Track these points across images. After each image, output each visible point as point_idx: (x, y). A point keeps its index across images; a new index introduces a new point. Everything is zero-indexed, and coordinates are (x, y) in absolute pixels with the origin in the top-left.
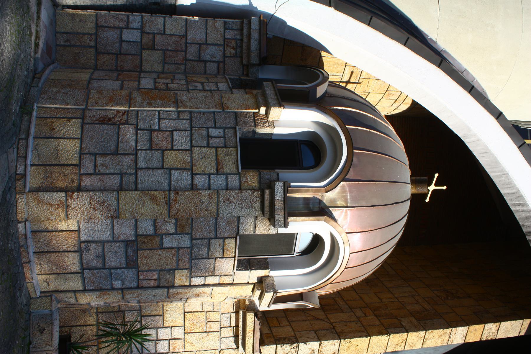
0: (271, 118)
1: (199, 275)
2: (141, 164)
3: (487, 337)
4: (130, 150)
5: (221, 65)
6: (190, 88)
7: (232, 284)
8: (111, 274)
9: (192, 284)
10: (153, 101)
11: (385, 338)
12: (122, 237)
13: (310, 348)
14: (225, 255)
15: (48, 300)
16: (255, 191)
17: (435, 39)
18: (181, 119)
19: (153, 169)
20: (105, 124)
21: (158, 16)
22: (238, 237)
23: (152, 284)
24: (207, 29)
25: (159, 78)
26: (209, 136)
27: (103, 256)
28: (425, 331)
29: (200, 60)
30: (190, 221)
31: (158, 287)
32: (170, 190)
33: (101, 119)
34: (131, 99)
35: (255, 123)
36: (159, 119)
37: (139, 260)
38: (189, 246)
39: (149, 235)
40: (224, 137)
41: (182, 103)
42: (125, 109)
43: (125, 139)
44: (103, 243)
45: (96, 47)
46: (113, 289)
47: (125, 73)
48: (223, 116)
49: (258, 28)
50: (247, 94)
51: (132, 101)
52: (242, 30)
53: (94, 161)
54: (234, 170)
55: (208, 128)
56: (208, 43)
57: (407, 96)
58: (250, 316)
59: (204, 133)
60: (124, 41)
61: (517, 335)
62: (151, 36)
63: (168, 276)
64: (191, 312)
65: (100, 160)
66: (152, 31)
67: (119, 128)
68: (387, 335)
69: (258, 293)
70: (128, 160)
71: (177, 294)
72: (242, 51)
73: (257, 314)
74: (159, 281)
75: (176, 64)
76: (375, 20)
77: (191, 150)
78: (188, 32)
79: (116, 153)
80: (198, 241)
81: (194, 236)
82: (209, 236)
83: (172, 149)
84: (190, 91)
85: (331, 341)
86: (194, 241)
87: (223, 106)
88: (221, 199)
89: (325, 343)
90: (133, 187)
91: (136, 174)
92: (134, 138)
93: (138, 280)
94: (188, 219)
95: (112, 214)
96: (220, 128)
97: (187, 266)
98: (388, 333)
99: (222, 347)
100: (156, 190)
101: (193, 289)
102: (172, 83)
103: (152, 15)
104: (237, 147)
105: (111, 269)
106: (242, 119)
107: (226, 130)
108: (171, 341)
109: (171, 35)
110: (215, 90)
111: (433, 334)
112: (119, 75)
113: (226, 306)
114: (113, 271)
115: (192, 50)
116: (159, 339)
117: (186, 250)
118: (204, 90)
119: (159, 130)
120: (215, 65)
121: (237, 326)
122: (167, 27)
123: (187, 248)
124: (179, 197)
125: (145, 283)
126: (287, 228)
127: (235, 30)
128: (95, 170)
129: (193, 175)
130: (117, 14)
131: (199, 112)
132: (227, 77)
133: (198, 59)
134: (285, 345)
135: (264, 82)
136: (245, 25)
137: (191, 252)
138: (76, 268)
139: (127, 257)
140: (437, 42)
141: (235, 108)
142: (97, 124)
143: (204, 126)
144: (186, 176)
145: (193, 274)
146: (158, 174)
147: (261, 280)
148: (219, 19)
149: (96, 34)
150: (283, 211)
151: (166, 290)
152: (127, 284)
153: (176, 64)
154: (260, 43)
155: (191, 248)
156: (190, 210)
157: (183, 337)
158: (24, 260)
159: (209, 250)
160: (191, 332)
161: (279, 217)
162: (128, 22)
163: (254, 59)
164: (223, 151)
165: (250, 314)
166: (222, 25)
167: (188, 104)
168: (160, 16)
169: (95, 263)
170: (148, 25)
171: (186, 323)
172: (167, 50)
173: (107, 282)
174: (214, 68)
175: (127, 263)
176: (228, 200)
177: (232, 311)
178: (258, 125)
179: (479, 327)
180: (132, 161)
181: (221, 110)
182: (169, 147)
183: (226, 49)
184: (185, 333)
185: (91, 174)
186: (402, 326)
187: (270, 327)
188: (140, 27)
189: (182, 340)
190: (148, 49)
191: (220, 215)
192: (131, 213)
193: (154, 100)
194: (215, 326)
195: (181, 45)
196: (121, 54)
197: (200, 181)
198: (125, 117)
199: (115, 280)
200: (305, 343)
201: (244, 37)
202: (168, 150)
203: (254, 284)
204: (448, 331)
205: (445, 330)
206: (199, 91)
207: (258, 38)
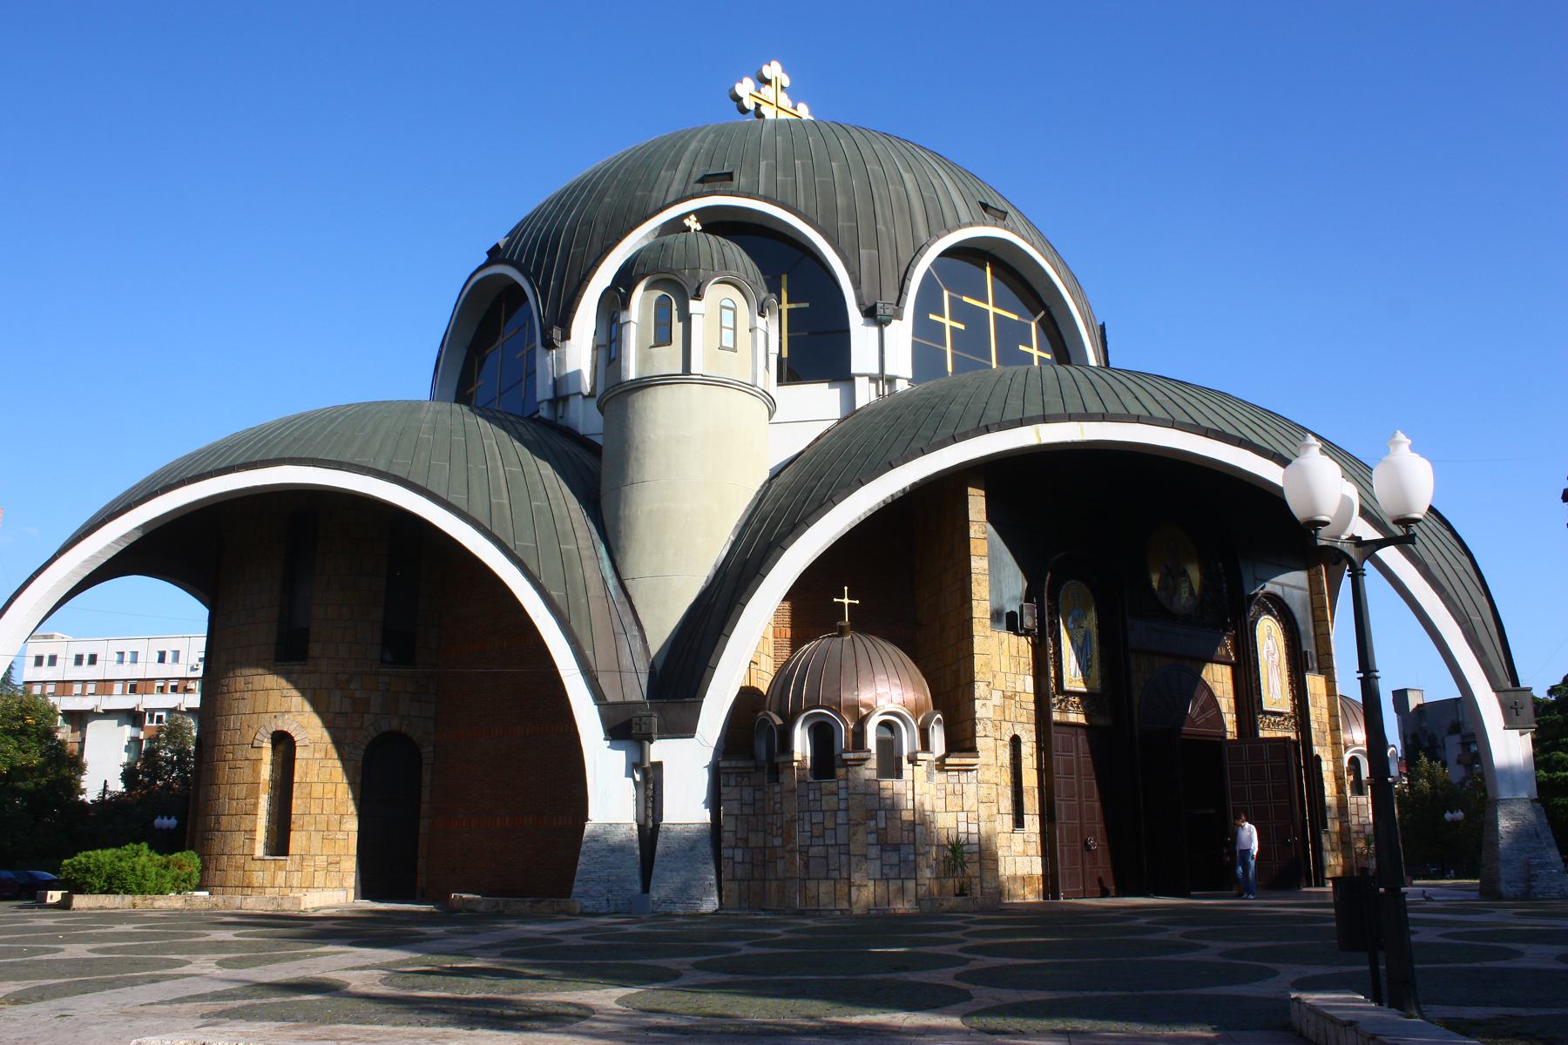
2: (833, 842)
7: (913, 781)
11: (976, 640)
12: (879, 853)
15: (922, 902)
23: (911, 835)
26: (814, 800)
29: (754, 804)
31: (914, 831)
32: (848, 824)
36: (804, 832)
44: (882, 865)
46: (915, 860)
52: (728, 773)
58: (948, 761)
61: (984, 499)
65: (831, 867)
69: (919, 763)
70: (830, 850)
72: (745, 773)
73: (947, 755)
77: (824, 812)
79: (826, 858)
87: (793, 791)
89: (977, 695)
90: (847, 847)
93: (909, 844)
105: (900, 861)
115: (746, 810)
118: (781, 802)
119: (811, 832)
121: (958, 770)
125: (911, 839)
129: (839, 810)
138: (899, 882)
139: (891, 851)
144: (840, 814)
147: (910, 761)
149: (739, 880)
152: (912, 850)
158: (893, 911)
161: (864, 755)
162: (729, 858)
163: (752, 763)
169: (896, 870)
194: (958, 787)
197: (843, 805)
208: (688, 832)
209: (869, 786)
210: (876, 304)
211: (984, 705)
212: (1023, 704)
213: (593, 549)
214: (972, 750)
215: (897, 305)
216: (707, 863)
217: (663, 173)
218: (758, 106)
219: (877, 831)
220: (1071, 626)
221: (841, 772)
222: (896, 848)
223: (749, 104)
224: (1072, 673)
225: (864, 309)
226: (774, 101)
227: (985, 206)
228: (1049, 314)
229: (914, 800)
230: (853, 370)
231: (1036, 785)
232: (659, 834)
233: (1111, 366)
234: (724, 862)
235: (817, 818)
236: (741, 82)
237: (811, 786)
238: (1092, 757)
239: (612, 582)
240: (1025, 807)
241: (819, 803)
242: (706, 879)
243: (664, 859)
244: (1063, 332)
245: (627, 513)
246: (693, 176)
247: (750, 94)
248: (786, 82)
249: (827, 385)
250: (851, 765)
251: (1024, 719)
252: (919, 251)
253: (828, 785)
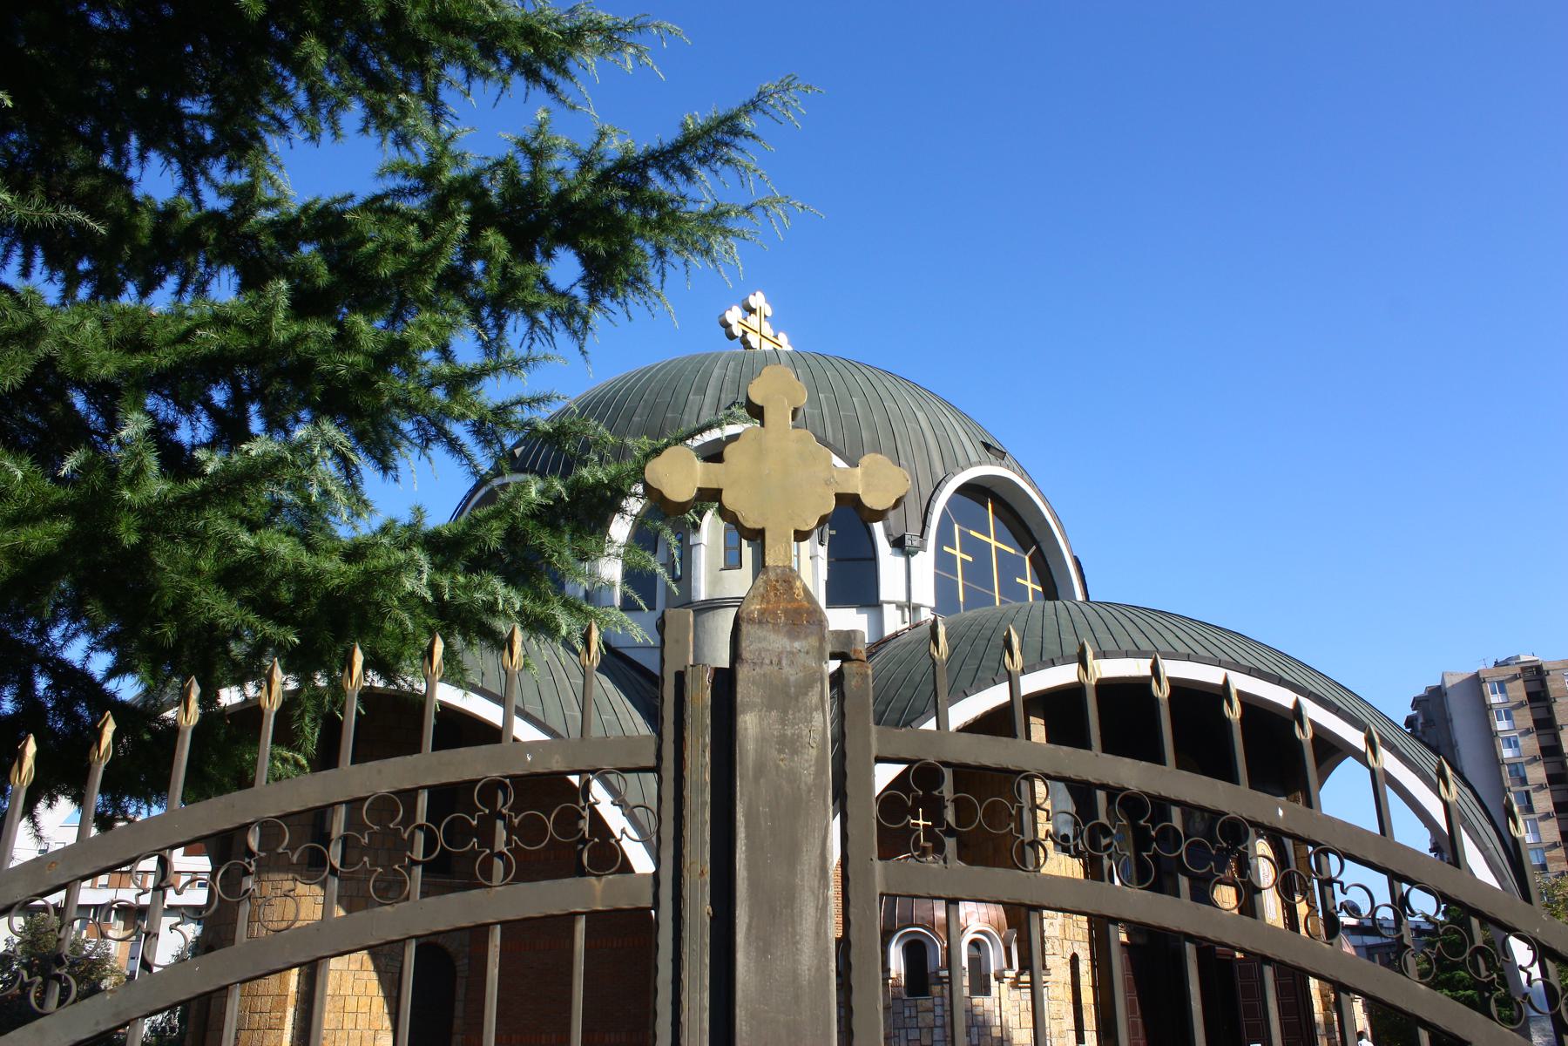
7: (1000, 998)
26: (910, 1017)
54: (930, 1001)
61: (1044, 727)
77: (920, 1029)
144: (937, 1031)
147: (997, 979)
182: (918, 1042)
197: (939, 1022)
203: (1000, 983)
210: (904, 536)
211: (1051, 924)
215: (921, 536)
217: (691, 397)
218: (745, 333)
221: (936, 989)
223: (737, 331)
225: (892, 539)
226: (758, 330)
227: (987, 446)
228: (1039, 549)
229: (1001, 1017)
230: (883, 596)
231: (1092, 1002)
233: (1091, 600)
235: (914, 1034)
236: (730, 309)
238: (1133, 975)
241: (914, 1019)
244: (1051, 566)
246: (723, 401)
247: (739, 322)
248: (769, 312)
249: (855, 609)
251: (1080, 938)
252: (937, 487)
253: (924, 1002)
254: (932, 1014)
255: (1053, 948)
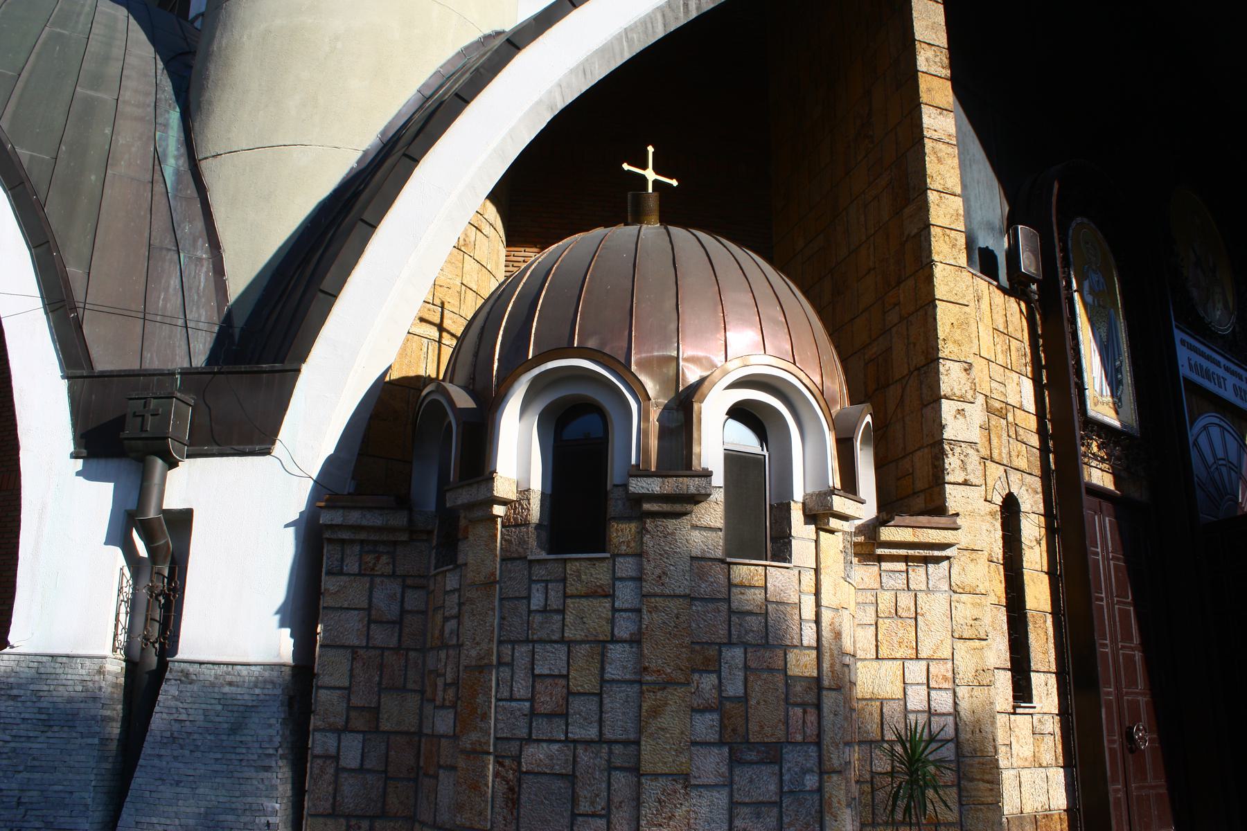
0: (513, 496)
1: (798, 632)
2: (593, 733)
3: (943, 67)
4: (568, 752)
5: (409, 581)
6: (454, 642)
7: (817, 571)
8: (791, 792)
9: (815, 645)
10: (479, 711)
11: (939, 271)
12: (724, 769)
13: (953, 418)
14: (762, 583)
16: (644, 528)
17: (360, 154)
18: (513, 660)
19: (601, 712)
20: (519, 799)
21: (316, 700)
22: (728, 560)
23: (812, 718)
24: (341, 608)
25: (434, 700)
26: (545, 610)
27: (758, 807)
28: (929, 191)
30: (697, 647)
31: (818, 706)
32: (640, 682)
33: (510, 804)
34: (474, 751)
35: (521, 525)
36: (511, 699)
37: (766, 740)
38: (742, 650)
39: (721, 721)
40: (547, 582)
41: (483, 658)
42: (492, 761)
43: (547, 761)
44: (733, 805)
45: (372, 818)
46: (820, 790)
47: (422, 764)
48: (508, 583)
49: (341, 512)
50: (467, 538)
51: (478, 748)
52: (343, 542)
53: (585, 819)
54: (605, 566)
55: (530, 612)
56: (366, 607)
57: (469, 223)
58: (887, 534)
59: (538, 618)
60: (362, 764)
62: (353, 714)
63: (798, 689)
64: (877, 646)
65: (584, 807)
66: (344, 713)
67: (527, 773)
68: (934, 267)
69: (834, 523)
70: (584, 757)
71: (832, 672)
73: (882, 520)
74: (808, 704)
75: (406, 667)
76: (326, 284)
77: (569, 643)
78: (346, 644)
79: (571, 778)
80: (733, 632)
81: (725, 641)
82: (724, 614)
83: (567, 677)
84: (460, 642)
85: (941, 376)
86: (734, 640)
87: (489, 583)
88: (657, 590)
89: (945, 388)
90: (633, 748)
91: (610, 742)
92: (545, 745)
93: (804, 743)
94: (693, 651)
95: (680, 786)
96: (529, 589)
97: (781, 653)
98: (930, 264)
99: (947, 588)
100: (640, 706)
101: (825, 642)
102: (444, 675)
103: (313, 712)
104: (565, 560)
105: (781, 793)
106: (514, 548)
107: (534, 578)
108: (931, 686)
109: (352, 676)
110: (459, 596)
111: (934, 175)
112: (426, 775)
113: (866, 579)
114: (786, 789)
115: (381, 636)
116: (926, 709)
117: (749, 655)
118: (458, 617)
119: (532, 700)
120: (410, 594)
122: (337, 684)
123: (746, 653)
124: (653, 666)
125: (811, 730)
126: (712, 472)
127: (343, 555)
128: (601, 816)
129: (614, 640)
130: (311, 777)
131: (501, 627)
132: (433, 572)
133: (398, 626)
134: (947, 466)
135: (445, 504)
136: (334, 536)
137: (754, 646)
139: (761, 762)
140: (364, 149)
141: (494, 561)
142: (518, 814)
143: (525, 618)
145: (796, 642)
146: (612, 702)
148: (323, 584)
149: (348, 817)
150: (681, 479)
151: (825, 693)
152: (812, 763)
153: (406, 667)
154: (370, 509)
155: (746, 646)
156: (677, 647)
157: (924, 663)
159: (750, 613)
160: (915, 647)
161: (692, 485)
162: (326, 757)
163: (400, 519)
164: (572, 585)
165: (882, 534)
166: (334, 579)
167: (484, 646)
168: (316, 696)
170: (332, 720)
171: (898, 656)
172: (380, 683)
173: (806, 799)
174: (416, 596)
175: (771, 763)
176: (660, 577)
177: (876, 568)
178: (526, 519)
179: (924, 83)
180: (586, 750)
181: (497, 586)
182: (563, 682)
183: (379, 573)
184: (917, 658)
185: (609, 823)
186: (918, 235)
187: (914, 493)
188: (336, 735)
189: (931, 663)
190: (378, 720)
191: (687, 591)
192: (679, 752)
193: (476, 708)
194: (906, 600)
195: (370, 658)
196: (385, 772)
197: (624, 628)
198: (507, 762)
199: (804, 785)
200: (944, 428)
201: (357, 537)
202: (568, 684)
203: (818, 530)
204: (929, 144)
205: (927, 151)
206: (461, 626)
207: (360, 512)
208: (230, 684)
209: (702, 576)
211: (960, 412)
212: (1021, 431)
213: (151, 109)
214: (936, 508)
216: (267, 769)
219: (720, 705)
220: (1089, 299)
221: (622, 533)
222: (773, 754)
224: (1097, 387)
231: (1048, 608)
232: (164, 687)
234: (312, 767)
235: (551, 661)
237: (538, 572)
239: (173, 162)
240: (1032, 655)
241: (558, 617)
242: (263, 812)
243: (163, 752)
245: (224, 42)
250: (654, 515)
254: (607, 604)
255: (964, 468)
